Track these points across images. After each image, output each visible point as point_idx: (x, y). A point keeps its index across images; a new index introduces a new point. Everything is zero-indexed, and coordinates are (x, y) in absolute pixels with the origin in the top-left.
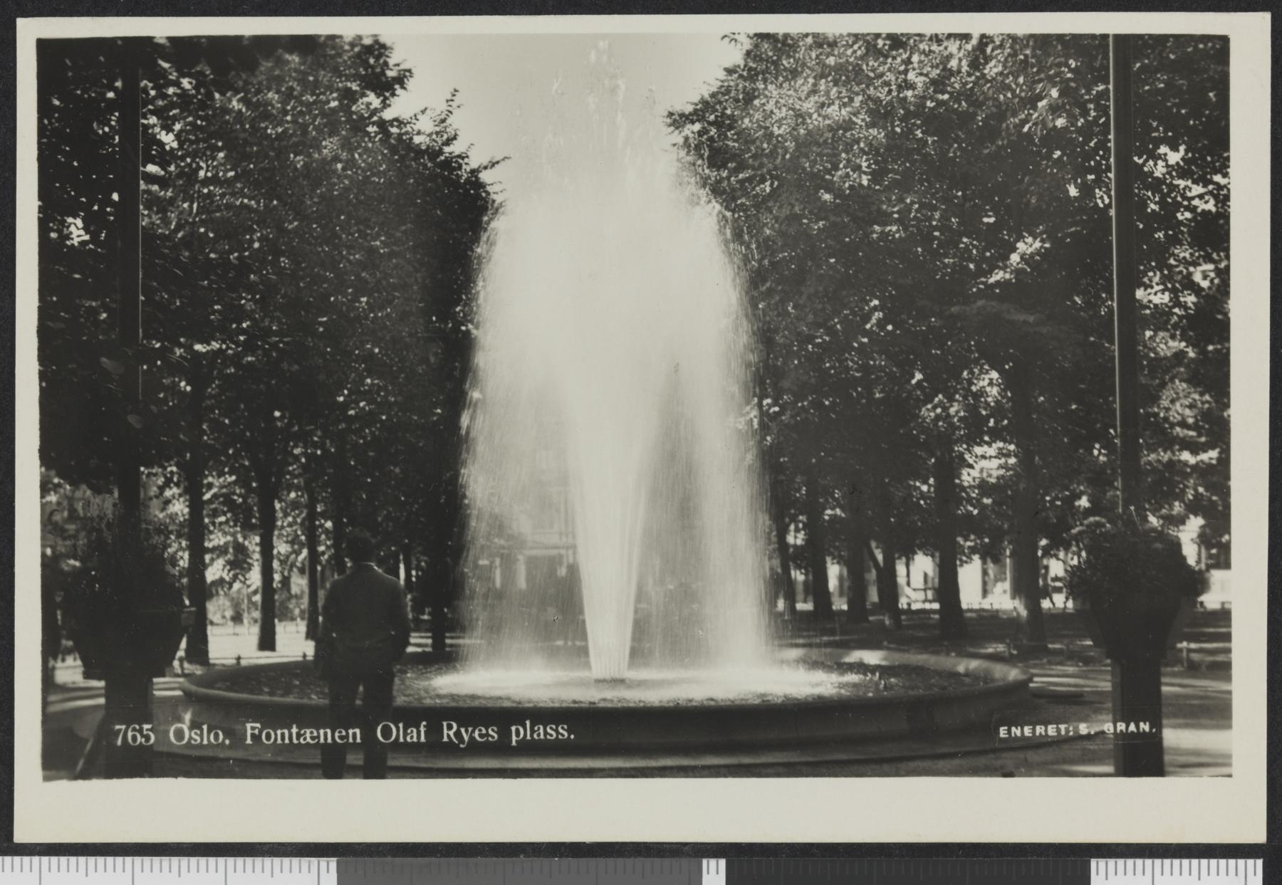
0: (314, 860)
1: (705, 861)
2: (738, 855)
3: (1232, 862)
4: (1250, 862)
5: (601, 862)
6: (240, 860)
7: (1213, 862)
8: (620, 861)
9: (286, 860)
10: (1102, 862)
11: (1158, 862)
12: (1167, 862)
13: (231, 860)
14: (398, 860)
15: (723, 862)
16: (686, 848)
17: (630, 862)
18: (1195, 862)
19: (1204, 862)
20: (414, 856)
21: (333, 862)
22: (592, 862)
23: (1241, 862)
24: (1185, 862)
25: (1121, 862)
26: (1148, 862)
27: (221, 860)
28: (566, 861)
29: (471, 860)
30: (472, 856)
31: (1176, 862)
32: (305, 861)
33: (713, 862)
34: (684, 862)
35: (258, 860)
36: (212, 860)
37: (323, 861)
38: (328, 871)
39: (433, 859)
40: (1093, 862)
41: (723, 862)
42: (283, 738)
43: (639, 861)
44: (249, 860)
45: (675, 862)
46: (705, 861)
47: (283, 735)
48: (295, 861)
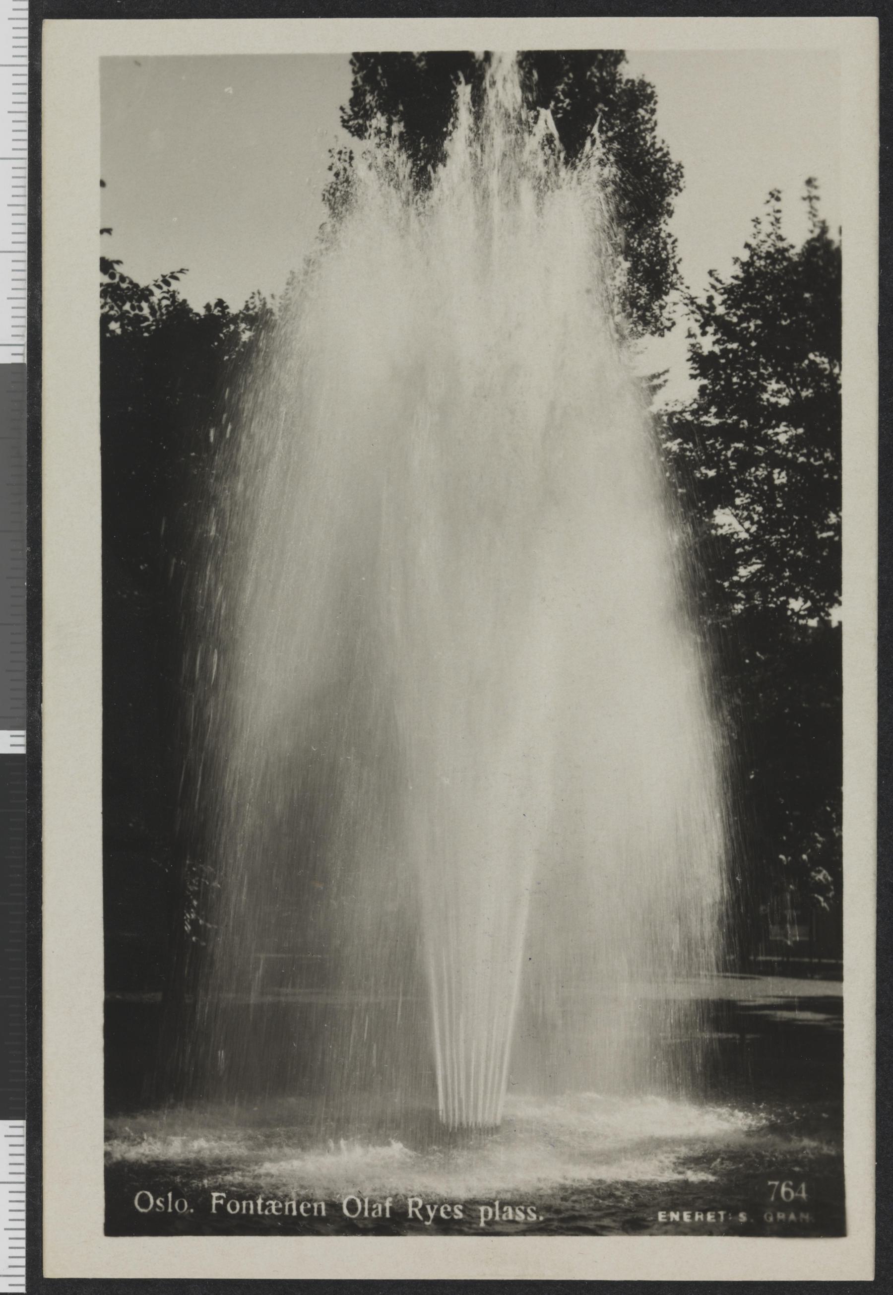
0: (24, 340)
1: (23, 733)
2: (31, 764)
3: (23, 1262)
4: (23, 1281)
5: (24, 629)
6: (24, 266)
7: (23, 1243)
8: (24, 648)
9: (24, 312)
10: (22, 1131)
11: (23, 1187)
12: (23, 1197)
13: (24, 257)
14: (24, 425)
15: (22, 750)
16: (36, 714)
17: (23, 657)
18: (23, 1225)
19: (23, 1234)
20: (29, 441)
21: (22, 359)
22: (23, 620)
23: (23, 1271)
24: (23, 1215)
25: (23, 1150)
26: (23, 1178)
27: (25, 247)
28: (24, 593)
29: (24, 498)
30: (28, 499)
31: (23, 1206)
32: (24, 331)
33: (23, 741)
34: (23, 712)
35: (25, 284)
36: (25, 238)
37: (23, 350)
38: (14, 354)
39: (25, 460)
40: (22, 1123)
41: (22, 750)
42: (248, 1209)
43: (24, 667)
44: (25, 275)
45: (23, 703)
46: (23, 733)
47: (248, 1205)
48: (24, 322)
